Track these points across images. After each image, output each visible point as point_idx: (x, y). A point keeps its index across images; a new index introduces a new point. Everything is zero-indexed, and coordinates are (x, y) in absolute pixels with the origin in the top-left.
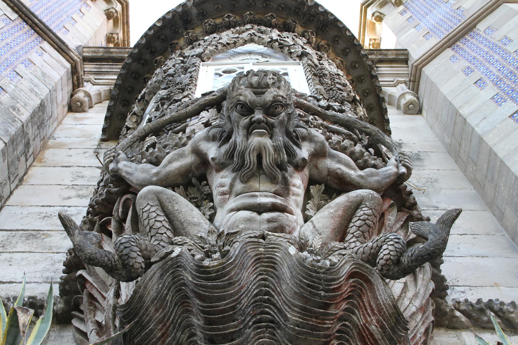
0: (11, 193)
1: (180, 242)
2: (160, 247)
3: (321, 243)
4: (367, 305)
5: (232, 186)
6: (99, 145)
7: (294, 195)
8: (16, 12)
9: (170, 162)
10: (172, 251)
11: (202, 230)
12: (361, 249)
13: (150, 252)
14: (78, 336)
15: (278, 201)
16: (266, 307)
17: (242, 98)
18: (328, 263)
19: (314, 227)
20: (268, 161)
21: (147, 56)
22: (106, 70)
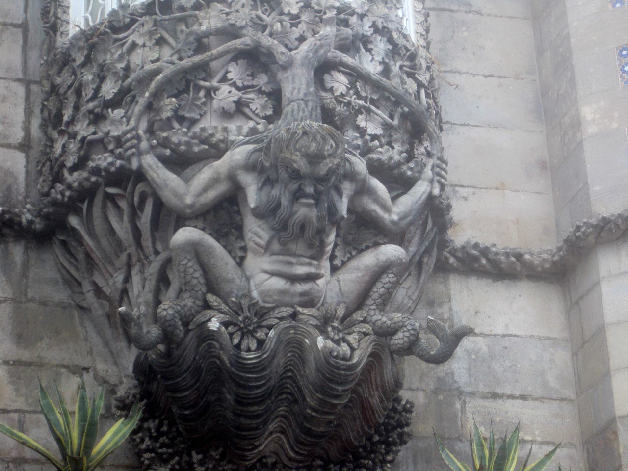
1: (215, 306)
2: (196, 306)
3: (343, 312)
4: (373, 380)
5: (269, 243)
9: (205, 190)
10: (209, 320)
11: (235, 287)
12: (379, 323)
13: (188, 318)
15: (313, 270)
16: (288, 383)
17: (295, 165)
18: (349, 352)
19: (340, 289)
20: (310, 235)
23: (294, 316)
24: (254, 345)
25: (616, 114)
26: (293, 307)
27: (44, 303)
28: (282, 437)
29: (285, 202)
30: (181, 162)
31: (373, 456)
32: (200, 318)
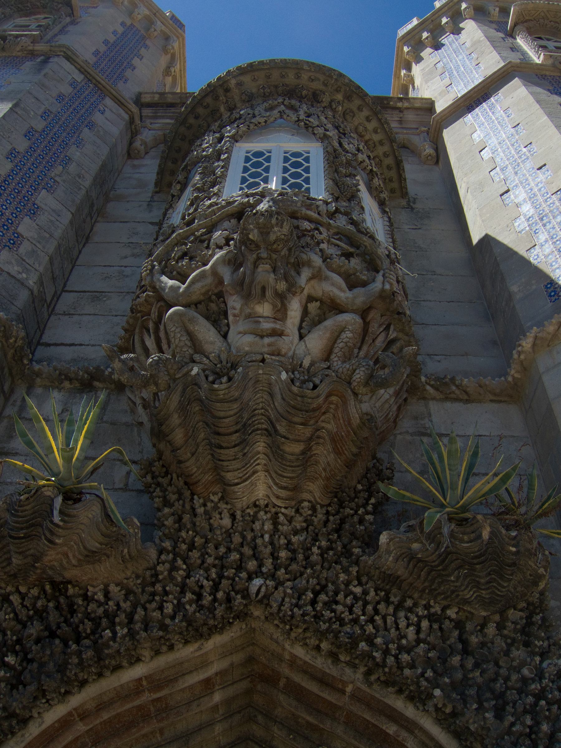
0: (80, 252)
4: (340, 416)
5: (241, 310)
6: (152, 197)
7: (291, 318)
8: (83, 73)
10: (192, 369)
12: (341, 369)
14: (130, 402)
15: (278, 327)
16: (262, 419)
17: (251, 236)
18: (311, 385)
19: (306, 346)
21: (191, 120)
22: (160, 114)
23: (263, 361)
24: (224, 379)
25: (534, 282)
26: (262, 354)
27: (113, 424)
28: (266, 474)
29: (248, 272)
30: (182, 278)
31: (356, 500)
32: (185, 370)
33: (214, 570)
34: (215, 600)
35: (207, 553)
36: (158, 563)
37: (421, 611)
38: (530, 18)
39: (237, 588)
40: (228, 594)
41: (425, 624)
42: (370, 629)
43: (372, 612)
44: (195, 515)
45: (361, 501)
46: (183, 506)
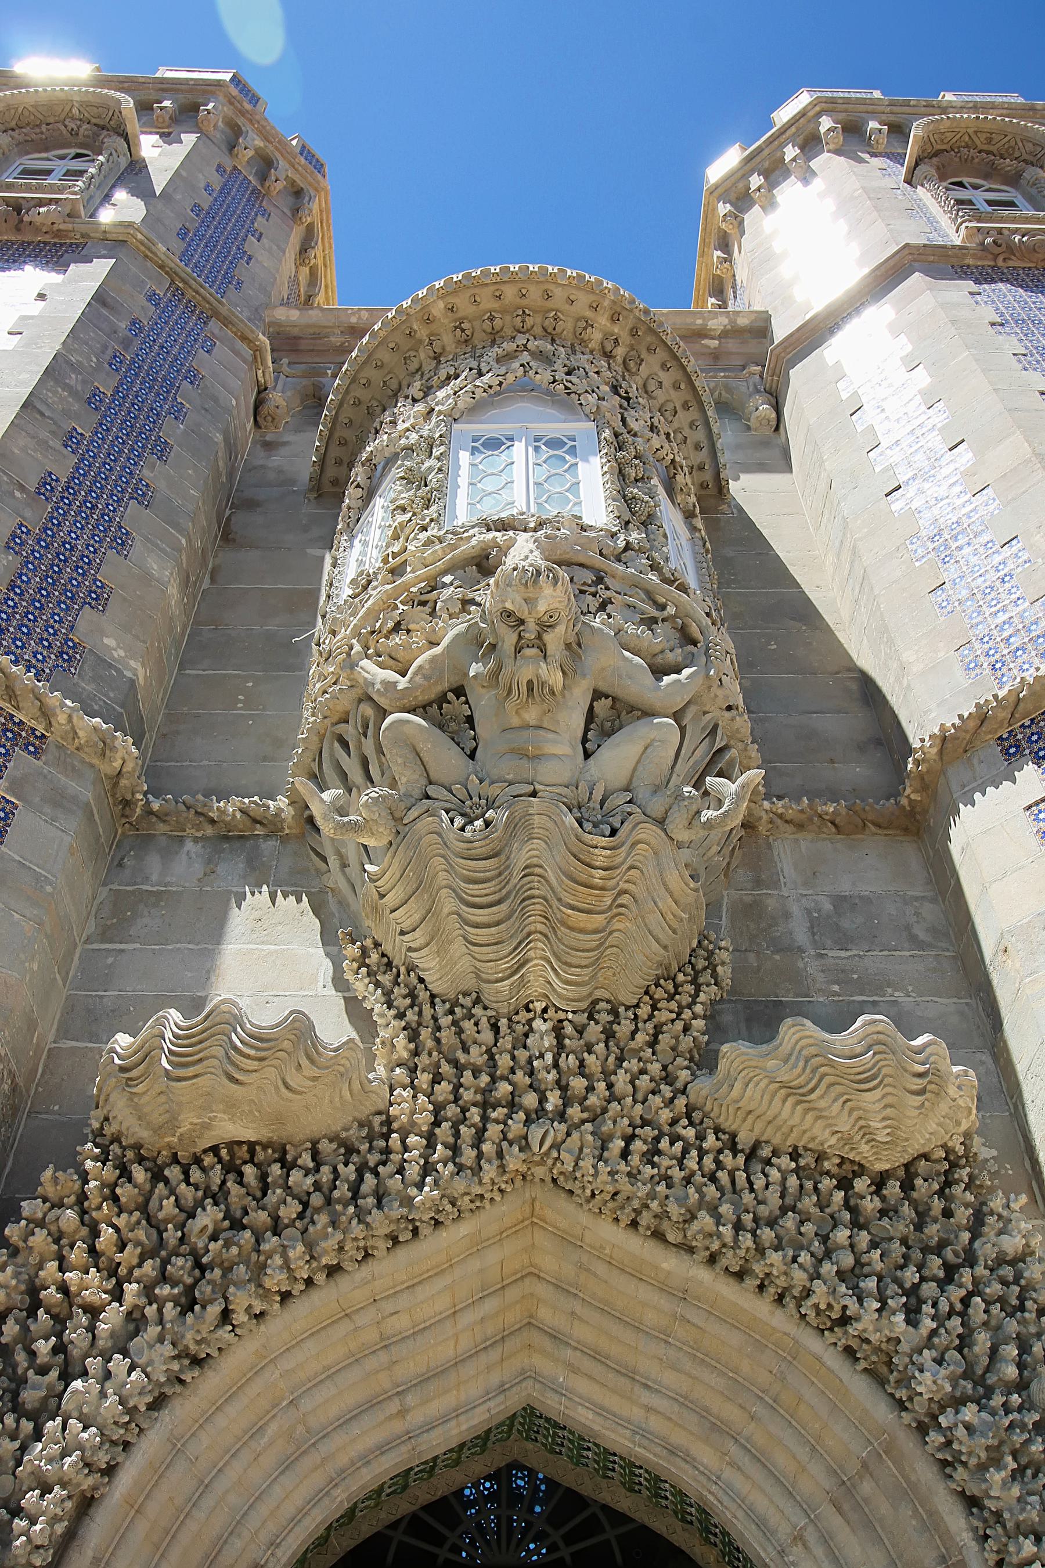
24: (479, 823)
25: (942, 644)
31: (677, 997)
33: (474, 1110)
34: (480, 1156)
35: (461, 1085)
36: (391, 1105)
37: (785, 1162)
38: (944, 147)
39: (510, 1136)
40: (499, 1145)
41: (793, 1181)
42: (711, 1190)
43: (713, 1166)
44: (439, 1029)
45: (686, 999)
46: (420, 1013)
